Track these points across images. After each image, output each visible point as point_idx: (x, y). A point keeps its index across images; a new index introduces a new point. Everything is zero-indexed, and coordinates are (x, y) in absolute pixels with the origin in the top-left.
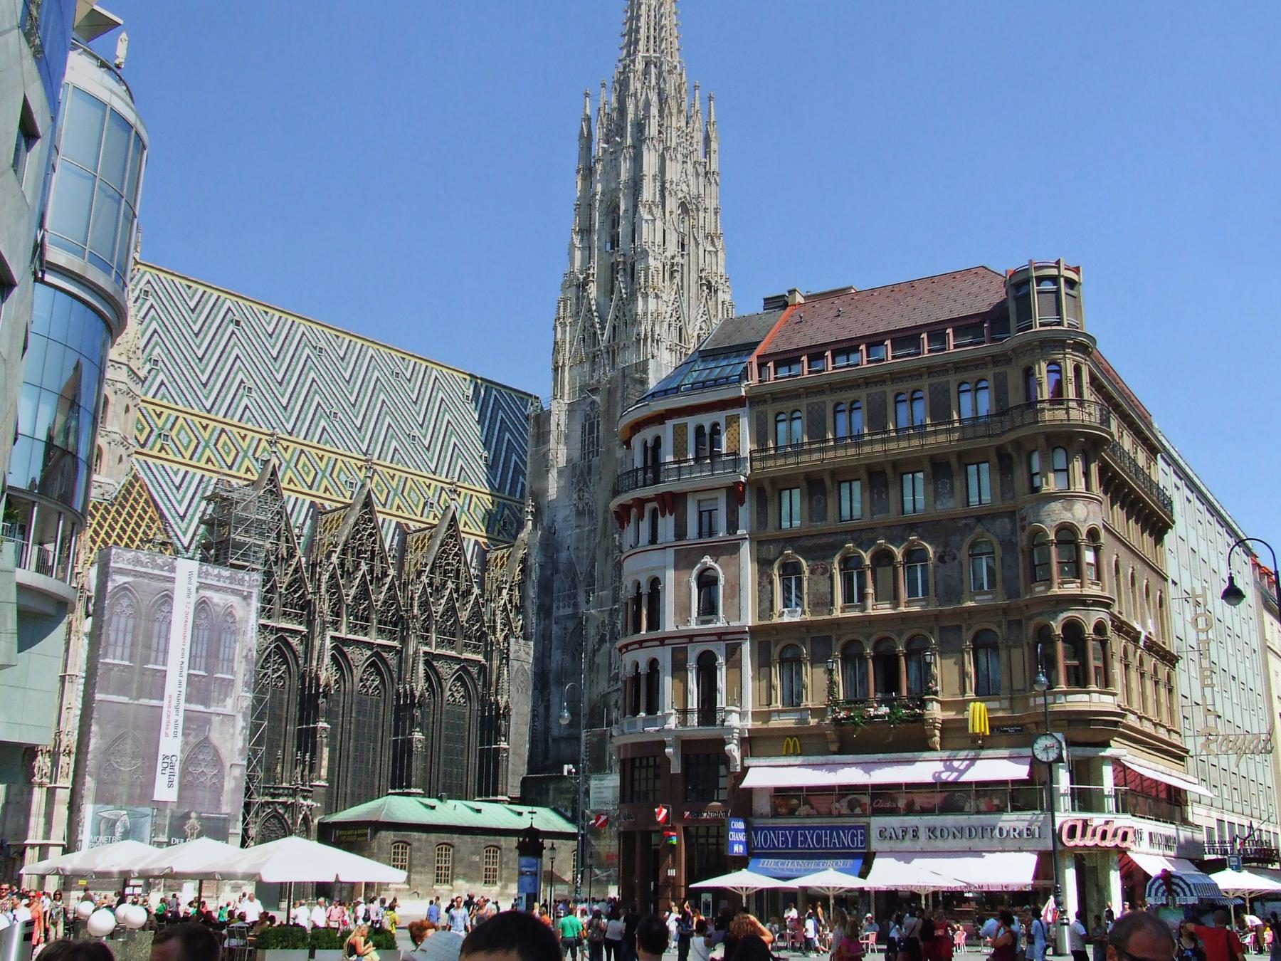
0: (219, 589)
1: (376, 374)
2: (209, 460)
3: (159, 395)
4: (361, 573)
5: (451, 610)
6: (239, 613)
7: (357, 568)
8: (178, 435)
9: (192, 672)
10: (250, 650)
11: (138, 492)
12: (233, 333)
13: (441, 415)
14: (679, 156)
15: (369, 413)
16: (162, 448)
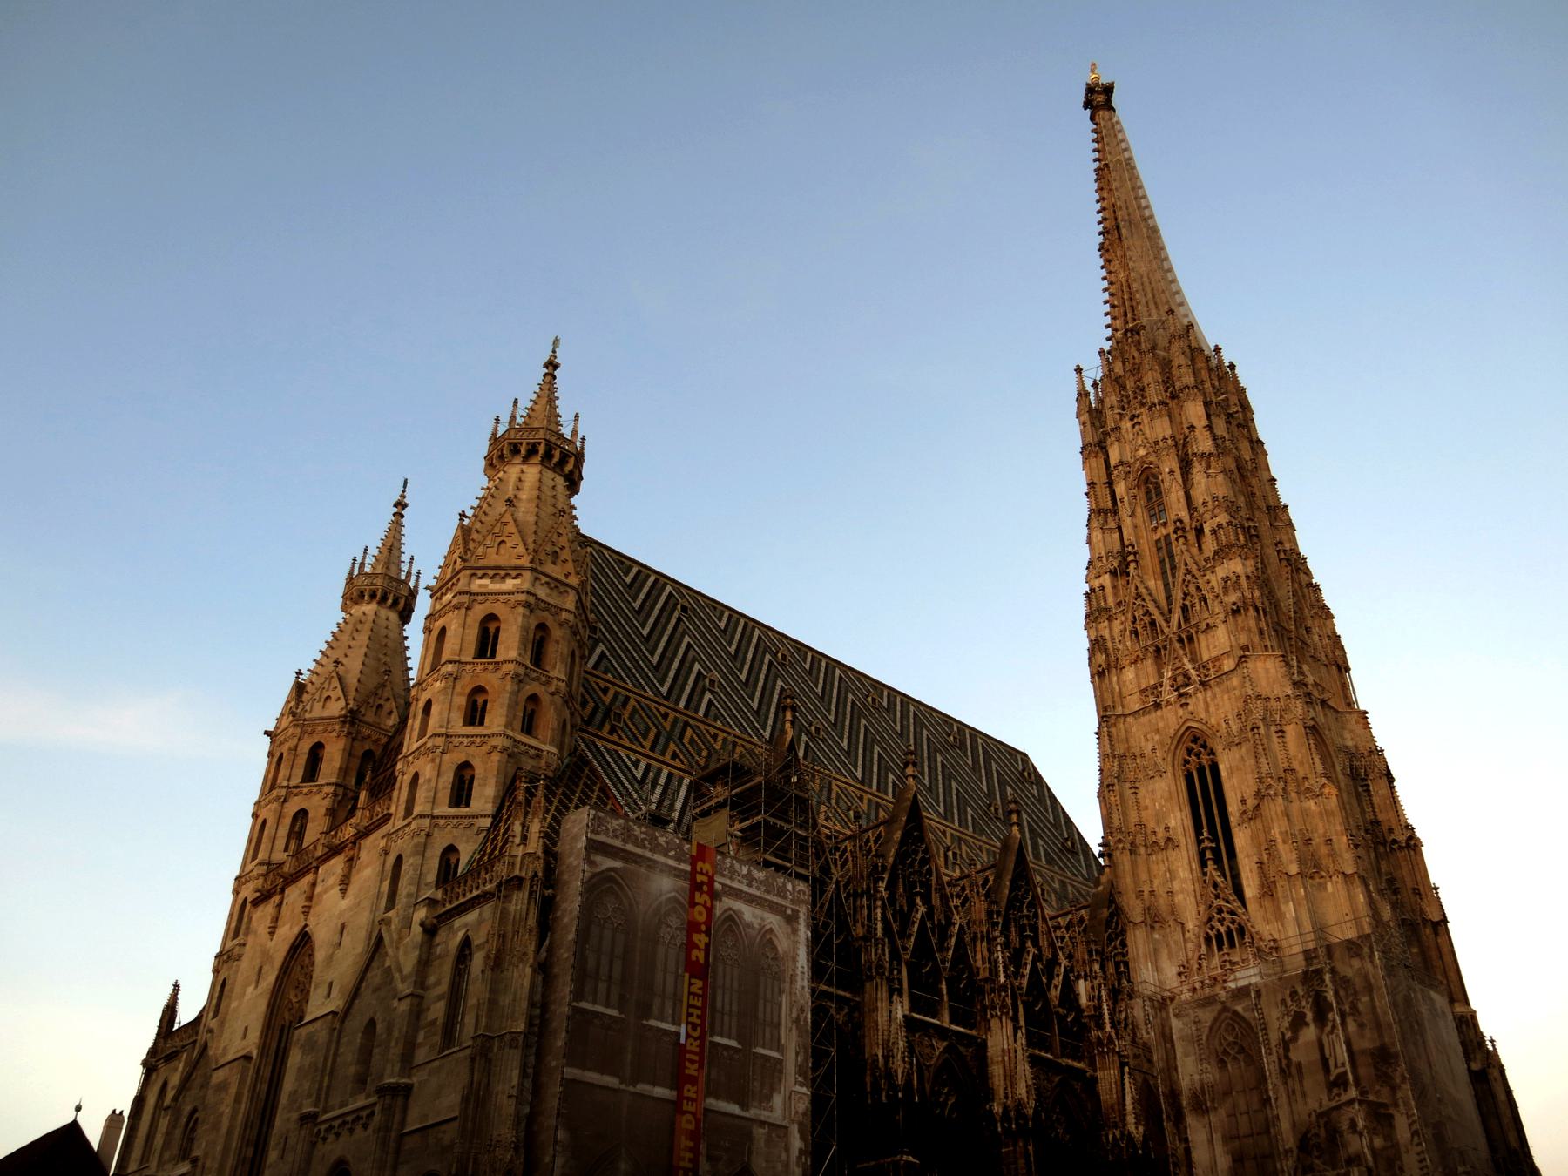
0: (751, 900)
1: (850, 696)
2: (674, 756)
3: (602, 668)
4: (919, 916)
5: (1038, 989)
6: (783, 944)
7: (912, 905)
8: (631, 718)
9: (717, 1039)
10: (802, 1010)
11: (590, 779)
12: (679, 620)
13: (932, 754)
14: (1223, 417)
15: (854, 737)
16: (613, 730)
